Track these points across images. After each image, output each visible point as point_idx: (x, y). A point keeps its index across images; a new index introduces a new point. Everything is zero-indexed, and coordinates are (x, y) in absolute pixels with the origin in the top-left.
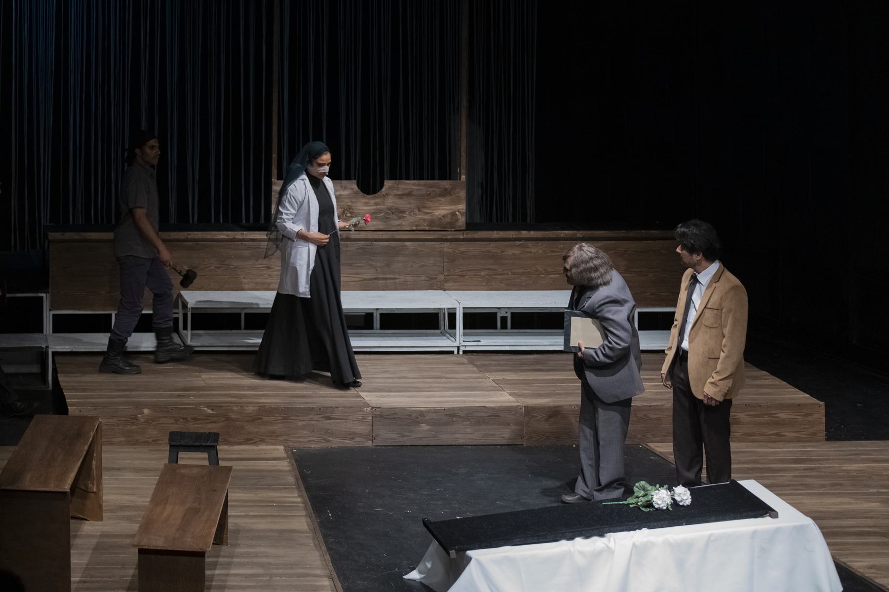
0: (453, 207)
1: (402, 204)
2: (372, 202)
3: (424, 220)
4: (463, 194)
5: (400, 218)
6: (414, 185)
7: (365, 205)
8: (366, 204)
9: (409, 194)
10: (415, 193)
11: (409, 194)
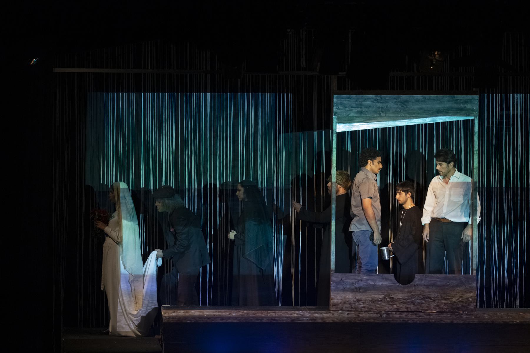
2: (406, 290)
3: (445, 304)
6: (438, 278)
10: (439, 283)
11: (434, 285)
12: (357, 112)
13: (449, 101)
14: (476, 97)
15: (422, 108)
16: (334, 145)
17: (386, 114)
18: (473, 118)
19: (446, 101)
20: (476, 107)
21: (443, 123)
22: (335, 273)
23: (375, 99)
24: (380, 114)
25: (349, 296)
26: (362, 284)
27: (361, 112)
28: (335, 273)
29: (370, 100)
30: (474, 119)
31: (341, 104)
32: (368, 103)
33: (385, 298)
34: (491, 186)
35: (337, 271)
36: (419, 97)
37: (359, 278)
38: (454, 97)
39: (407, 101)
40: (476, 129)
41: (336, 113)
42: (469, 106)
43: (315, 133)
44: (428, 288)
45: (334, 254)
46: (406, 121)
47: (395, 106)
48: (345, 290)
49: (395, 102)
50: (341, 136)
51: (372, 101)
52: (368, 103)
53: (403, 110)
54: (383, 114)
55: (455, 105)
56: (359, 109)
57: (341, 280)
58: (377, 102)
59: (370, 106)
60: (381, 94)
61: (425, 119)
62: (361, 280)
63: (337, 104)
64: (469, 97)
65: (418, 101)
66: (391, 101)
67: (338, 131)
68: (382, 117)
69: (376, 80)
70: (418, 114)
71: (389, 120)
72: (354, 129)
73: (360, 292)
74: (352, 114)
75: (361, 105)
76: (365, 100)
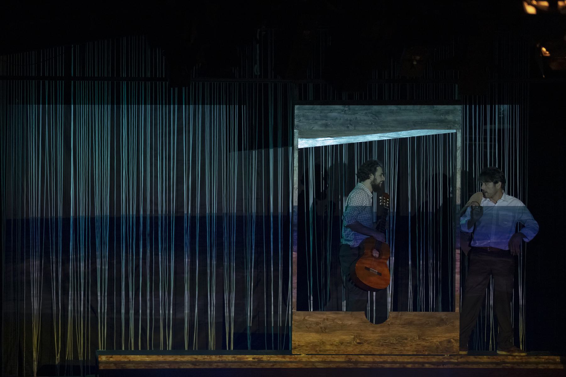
0: (448, 335)
2: (379, 330)
4: (457, 323)
7: (373, 333)
8: (373, 332)
9: (410, 323)
11: (410, 323)
14: (459, 107)
17: (355, 126)
18: (455, 131)
21: (419, 138)
22: (298, 310)
23: (342, 111)
24: (348, 127)
25: (313, 337)
26: (328, 323)
27: (326, 125)
28: (298, 310)
29: (336, 112)
30: (456, 133)
31: (303, 116)
33: (354, 338)
36: (393, 107)
37: (325, 317)
38: (434, 107)
39: (379, 112)
41: (298, 126)
42: (450, 117)
46: (378, 135)
47: (366, 118)
48: (309, 329)
49: (366, 113)
50: (304, 152)
51: (339, 113)
54: (351, 128)
56: (324, 122)
57: (304, 320)
58: (345, 113)
59: (337, 119)
61: (400, 132)
62: (327, 319)
63: (299, 116)
64: (451, 107)
65: (392, 112)
66: (361, 112)
67: (300, 147)
70: (392, 127)
71: (358, 135)
72: (318, 145)
73: (326, 333)
74: (316, 128)
75: (327, 117)
76: (331, 111)
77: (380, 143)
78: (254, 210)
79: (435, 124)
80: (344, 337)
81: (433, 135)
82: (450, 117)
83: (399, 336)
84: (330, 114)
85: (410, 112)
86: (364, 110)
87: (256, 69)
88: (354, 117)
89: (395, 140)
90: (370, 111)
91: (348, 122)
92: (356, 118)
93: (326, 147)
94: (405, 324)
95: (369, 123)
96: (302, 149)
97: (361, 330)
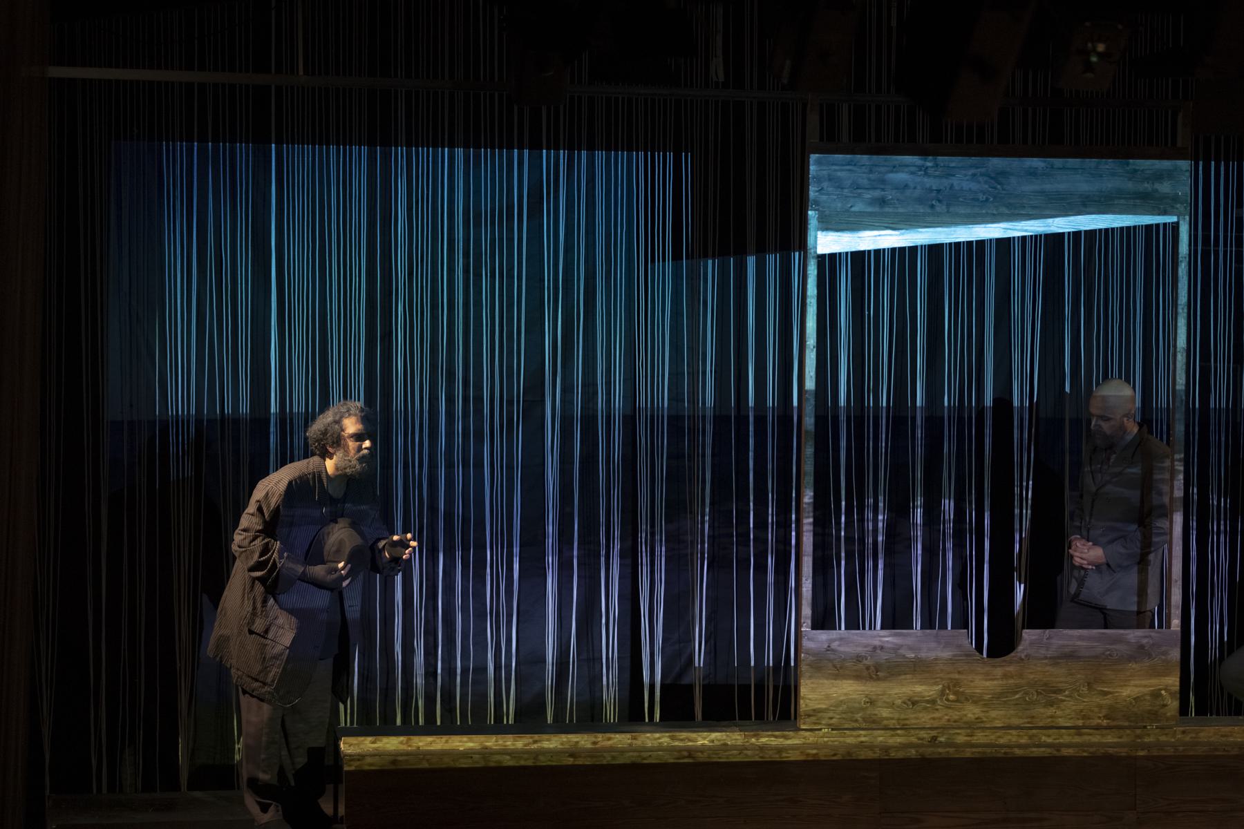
1: (1058, 675)
2: (999, 672)
3: (1100, 707)
5: (1051, 704)
6: (1081, 638)
7: (986, 679)
12: (873, 202)
13: (1113, 174)
14: (1185, 165)
15: (1042, 192)
16: (812, 290)
17: (948, 206)
18: (1174, 219)
19: (1108, 173)
20: (1184, 188)
21: (1091, 234)
23: (920, 168)
24: (932, 206)
25: (848, 689)
26: (883, 657)
27: (883, 202)
28: (814, 627)
29: (905, 170)
30: (1178, 223)
31: (830, 180)
32: (901, 176)
33: (942, 693)
34: (1212, 405)
35: (815, 626)
36: (1037, 163)
38: (1128, 164)
39: (1004, 174)
40: (1184, 248)
41: (817, 203)
42: (1165, 188)
43: (751, 261)
44: (1056, 664)
45: (810, 581)
47: (974, 186)
49: (974, 175)
50: (829, 263)
51: (912, 173)
52: (901, 176)
53: (995, 197)
54: (940, 208)
55: (1130, 186)
56: (877, 193)
58: (926, 174)
59: (906, 186)
60: (936, 154)
61: (1050, 221)
62: (882, 648)
64: (1166, 164)
65: (1033, 173)
66: (962, 173)
67: (820, 251)
68: (939, 214)
69: (933, 110)
70: (1034, 207)
71: (956, 224)
73: (878, 679)
75: (883, 181)
76: (894, 169)
77: (1003, 244)
78: (710, 402)
79: (1132, 202)
80: (919, 688)
81: (1122, 228)
82: (1165, 188)
83: (1046, 684)
84: (891, 176)
85: (1074, 174)
86: (971, 167)
87: (717, 69)
88: (946, 182)
89: (1036, 238)
90: (983, 170)
91: (934, 194)
92: (952, 187)
93: (877, 252)
94: (1058, 658)
95: (982, 197)
96: (824, 255)
97: (959, 672)
